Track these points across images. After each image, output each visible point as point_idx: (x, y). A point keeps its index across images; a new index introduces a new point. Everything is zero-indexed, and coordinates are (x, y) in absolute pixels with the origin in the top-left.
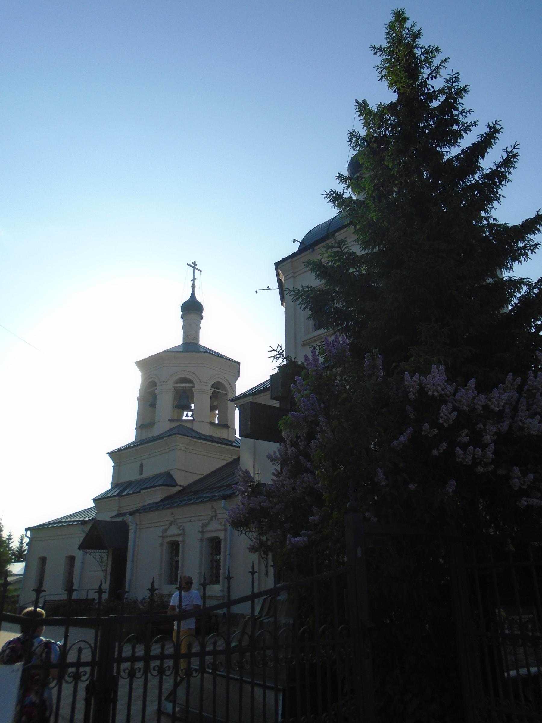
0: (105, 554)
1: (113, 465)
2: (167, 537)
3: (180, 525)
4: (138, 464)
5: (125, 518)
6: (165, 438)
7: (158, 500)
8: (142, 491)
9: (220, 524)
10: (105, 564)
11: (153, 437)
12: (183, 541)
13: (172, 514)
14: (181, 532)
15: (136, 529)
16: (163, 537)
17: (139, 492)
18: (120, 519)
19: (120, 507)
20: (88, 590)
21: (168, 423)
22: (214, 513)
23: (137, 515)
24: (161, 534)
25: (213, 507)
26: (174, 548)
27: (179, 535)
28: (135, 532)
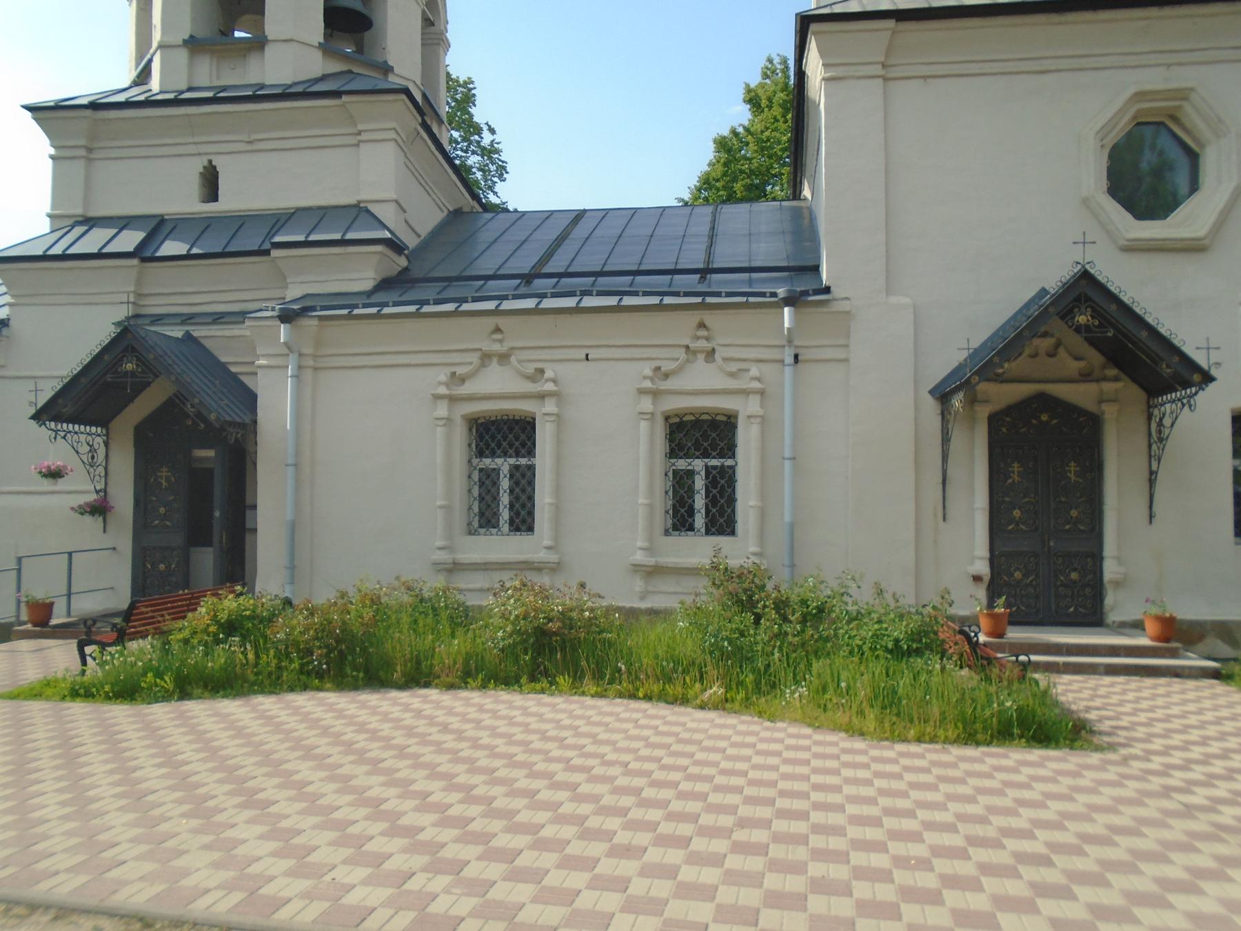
0: (99, 440)
1: (52, 151)
2: (471, 398)
3: (530, 369)
4: (196, 166)
5: (198, 332)
6: (345, 98)
7: (368, 285)
8: (275, 253)
9: (732, 375)
10: (101, 470)
11: (262, 86)
12: (559, 419)
13: (498, 330)
14: (550, 387)
15: (300, 367)
16: (453, 399)
17: (266, 253)
18: (177, 332)
19: (139, 295)
20: (70, 554)
21: (318, 55)
22: (702, 344)
23: (309, 323)
24: (443, 390)
25: (702, 325)
26: (503, 435)
27: (542, 396)
28: (296, 377)
